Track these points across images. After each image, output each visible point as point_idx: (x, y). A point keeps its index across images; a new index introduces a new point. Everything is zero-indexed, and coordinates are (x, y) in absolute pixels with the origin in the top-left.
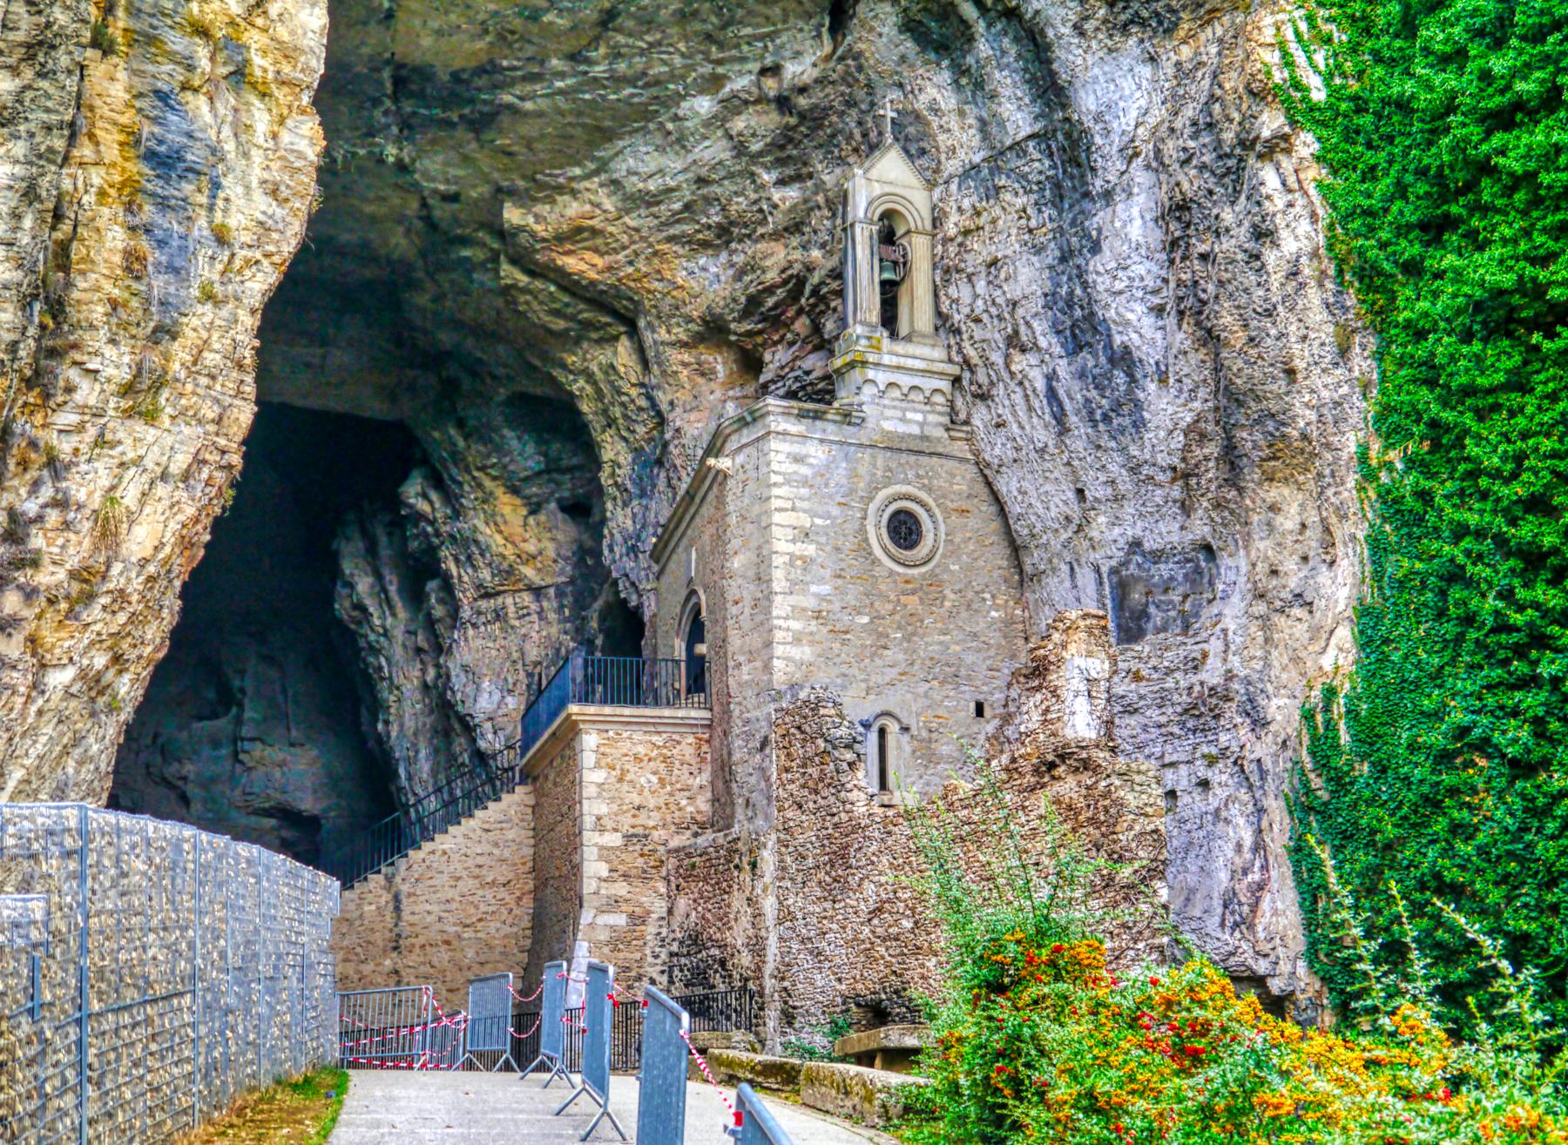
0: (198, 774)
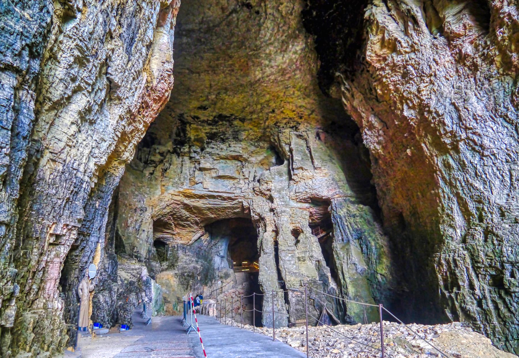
0: (275, 187)
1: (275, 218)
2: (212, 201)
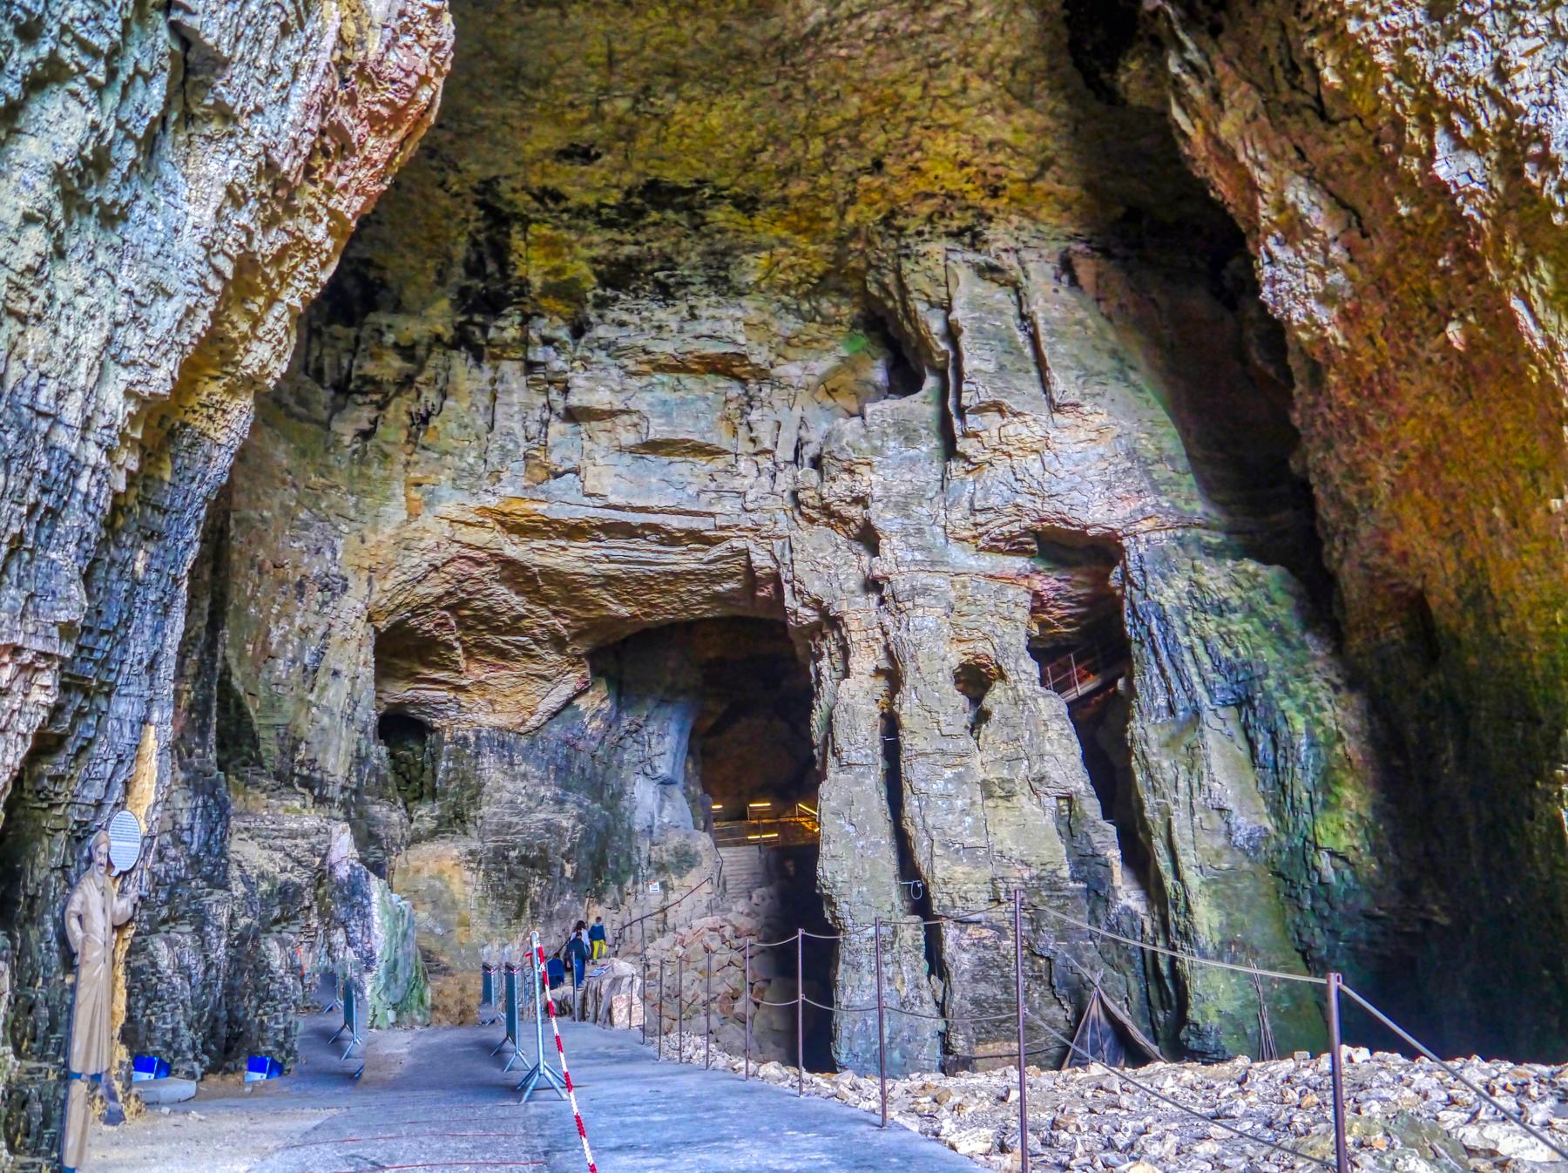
0: (886, 488)
1: (888, 620)
2: (619, 547)
